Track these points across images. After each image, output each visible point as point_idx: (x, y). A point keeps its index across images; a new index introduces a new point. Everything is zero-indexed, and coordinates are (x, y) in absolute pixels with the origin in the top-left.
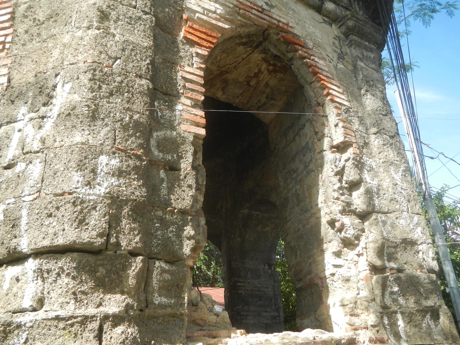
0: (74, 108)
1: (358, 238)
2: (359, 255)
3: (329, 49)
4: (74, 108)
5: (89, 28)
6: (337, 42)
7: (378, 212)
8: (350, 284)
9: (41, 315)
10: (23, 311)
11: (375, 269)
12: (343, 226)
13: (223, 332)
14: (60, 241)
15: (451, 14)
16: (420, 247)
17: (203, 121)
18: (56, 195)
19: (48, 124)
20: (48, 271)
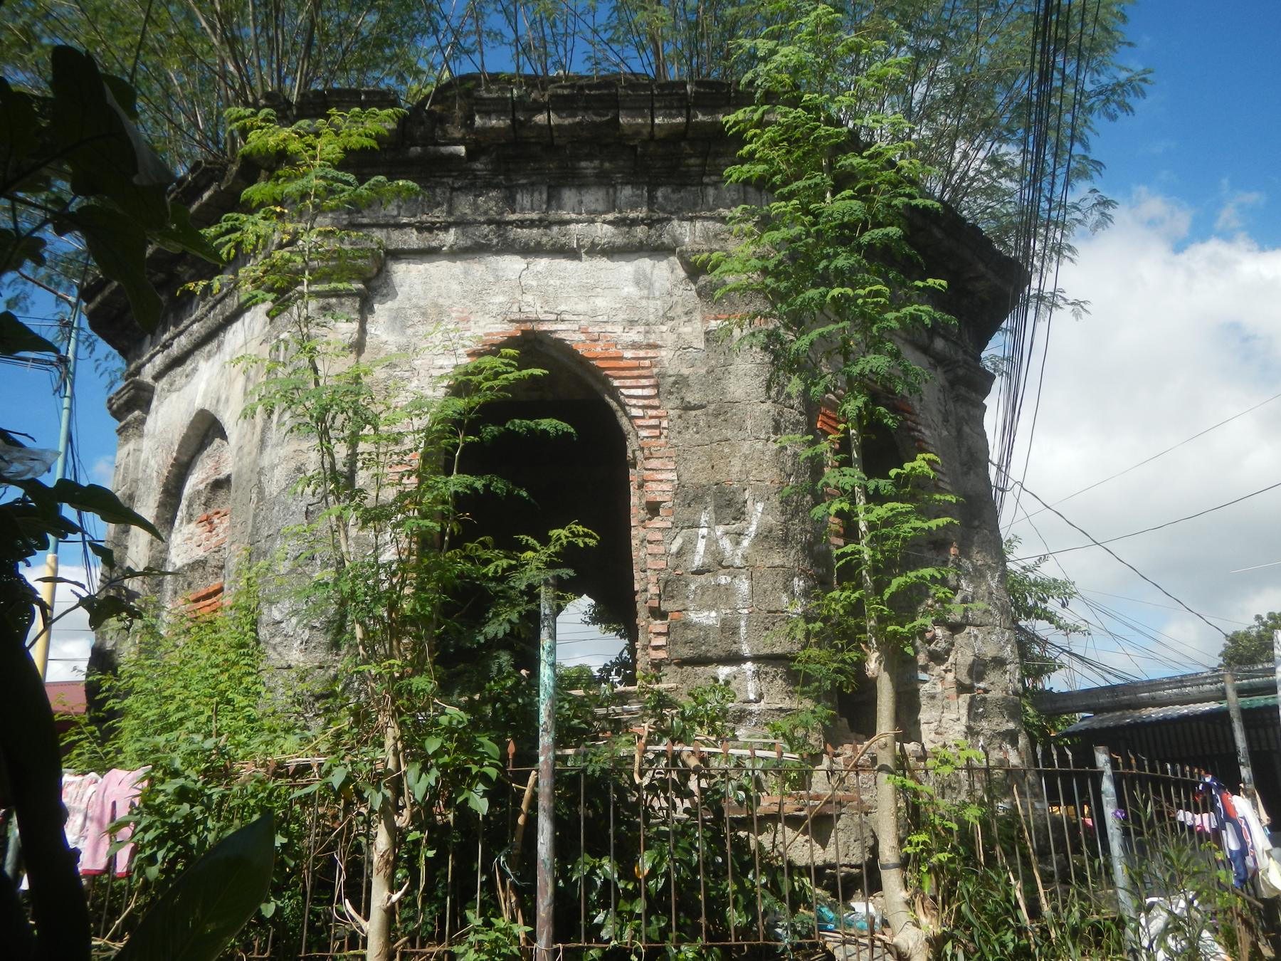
0: (770, 531)
1: (948, 652)
2: (946, 671)
4: (770, 531)
5: (768, 440)
7: (970, 625)
8: (935, 701)
9: (762, 705)
10: (750, 702)
11: (962, 688)
12: (934, 637)
13: (852, 735)
14: (778, 650)
15: (1077, 315)
17: (842, 531)
18: (769, 612)
19: (746, 543)
20: (766, 673)
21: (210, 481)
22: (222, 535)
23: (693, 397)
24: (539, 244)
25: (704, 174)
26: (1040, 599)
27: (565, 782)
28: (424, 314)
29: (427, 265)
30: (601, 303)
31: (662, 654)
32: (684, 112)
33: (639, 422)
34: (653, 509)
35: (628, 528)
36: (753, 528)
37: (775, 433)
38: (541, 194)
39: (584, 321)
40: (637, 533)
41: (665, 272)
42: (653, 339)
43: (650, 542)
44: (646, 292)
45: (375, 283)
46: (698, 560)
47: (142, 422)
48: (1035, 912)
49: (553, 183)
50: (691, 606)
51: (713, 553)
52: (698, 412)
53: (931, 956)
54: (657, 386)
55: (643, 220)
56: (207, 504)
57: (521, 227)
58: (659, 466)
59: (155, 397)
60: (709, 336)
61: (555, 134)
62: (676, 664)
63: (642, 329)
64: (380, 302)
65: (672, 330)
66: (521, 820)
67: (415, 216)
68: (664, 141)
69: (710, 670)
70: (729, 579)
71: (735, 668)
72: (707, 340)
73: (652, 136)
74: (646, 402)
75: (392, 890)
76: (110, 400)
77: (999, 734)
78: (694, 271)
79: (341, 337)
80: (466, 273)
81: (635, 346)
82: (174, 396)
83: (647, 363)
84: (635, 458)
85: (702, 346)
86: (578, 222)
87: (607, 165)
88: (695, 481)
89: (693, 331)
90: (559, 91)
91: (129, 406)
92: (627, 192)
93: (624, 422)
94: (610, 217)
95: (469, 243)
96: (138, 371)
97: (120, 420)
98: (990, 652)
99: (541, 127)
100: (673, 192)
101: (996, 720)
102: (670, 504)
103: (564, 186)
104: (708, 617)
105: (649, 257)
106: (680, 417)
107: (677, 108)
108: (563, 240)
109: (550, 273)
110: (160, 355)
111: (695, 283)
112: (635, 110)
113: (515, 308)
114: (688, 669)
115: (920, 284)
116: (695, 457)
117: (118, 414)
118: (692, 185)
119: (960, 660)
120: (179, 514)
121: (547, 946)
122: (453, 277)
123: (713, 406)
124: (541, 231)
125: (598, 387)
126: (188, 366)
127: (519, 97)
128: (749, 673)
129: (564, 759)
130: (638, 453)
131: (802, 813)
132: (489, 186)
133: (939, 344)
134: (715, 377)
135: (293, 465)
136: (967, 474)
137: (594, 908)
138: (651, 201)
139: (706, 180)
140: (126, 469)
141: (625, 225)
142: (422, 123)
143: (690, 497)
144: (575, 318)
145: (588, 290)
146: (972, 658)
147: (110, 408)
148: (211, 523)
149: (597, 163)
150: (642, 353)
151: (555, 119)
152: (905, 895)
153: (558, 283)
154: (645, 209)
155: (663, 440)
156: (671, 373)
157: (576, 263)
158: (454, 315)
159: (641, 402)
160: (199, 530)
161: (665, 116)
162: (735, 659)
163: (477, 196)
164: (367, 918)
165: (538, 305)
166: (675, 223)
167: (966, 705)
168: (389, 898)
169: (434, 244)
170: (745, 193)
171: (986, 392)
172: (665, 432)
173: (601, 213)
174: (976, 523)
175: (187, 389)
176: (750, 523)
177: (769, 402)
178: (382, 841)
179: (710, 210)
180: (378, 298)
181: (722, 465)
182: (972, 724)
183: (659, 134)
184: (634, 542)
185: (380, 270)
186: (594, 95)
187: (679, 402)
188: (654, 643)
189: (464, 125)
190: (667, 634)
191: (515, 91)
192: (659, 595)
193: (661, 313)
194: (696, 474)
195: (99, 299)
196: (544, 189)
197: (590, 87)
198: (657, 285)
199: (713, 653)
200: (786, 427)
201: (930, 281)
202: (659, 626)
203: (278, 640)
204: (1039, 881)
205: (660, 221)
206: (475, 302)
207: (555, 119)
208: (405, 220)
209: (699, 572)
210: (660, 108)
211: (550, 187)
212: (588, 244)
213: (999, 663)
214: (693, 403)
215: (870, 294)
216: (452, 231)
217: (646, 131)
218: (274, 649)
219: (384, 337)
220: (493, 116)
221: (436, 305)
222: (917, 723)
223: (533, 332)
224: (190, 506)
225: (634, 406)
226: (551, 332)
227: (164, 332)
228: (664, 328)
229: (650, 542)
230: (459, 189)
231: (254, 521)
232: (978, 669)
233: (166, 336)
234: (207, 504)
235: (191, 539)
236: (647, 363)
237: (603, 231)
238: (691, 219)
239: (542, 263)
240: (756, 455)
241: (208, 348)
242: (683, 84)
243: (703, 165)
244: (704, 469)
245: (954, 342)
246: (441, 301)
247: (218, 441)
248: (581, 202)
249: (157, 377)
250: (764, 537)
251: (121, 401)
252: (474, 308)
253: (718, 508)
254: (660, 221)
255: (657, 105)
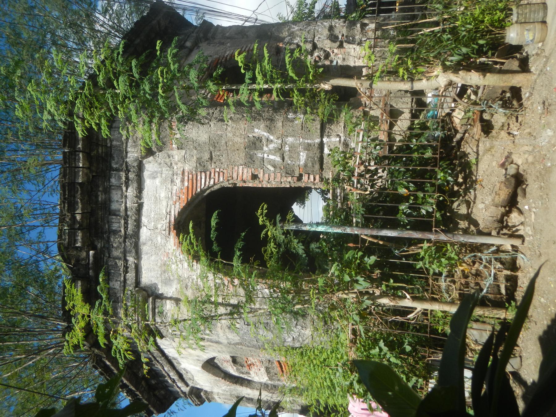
0: (267, 126)
1: (325, 51)
2: (333, 53)
3: (218, 48)
4: (267, 126)
5: (227, 125)
6: (212, 45)
7: (314, 40)
8: (346, 58)
10: (340, 140)
11: (341, 46)
12: (318, 56)
14: (319, 127)
16: (333, 24)
18: (302, 129)
19: (272, 138)
20: (328, 132)
21: (232, 364)
22: (256, 360)
23: (207, 156)
24: (135, 220)
25: (106, 146)
26: (306, 6)
27: (366, 223)
28: (164, 272)
29: (143, 270)
30: (163, 195)
31: (317, 177)
32: (77, 153)
33: (216, 181)
34: (255, 177)
35: (262, 188)
36: (265, 134)
37: (224, 121)
38: (113, 219)
39: (171, 202)
40: (265, 185)
41: (150, 166)
42: (180, 172)
43: (269, 179)
44: (159, 175)
45: (150, 292)
46: (278, 159)
47: (206, 392)
48: (437, 24)
49: (108, 213)
50: (298, 163)
51: (275, 152)
52: (213, 155)
53: (451, 71)
54: (201, 172)
55: (126, 174)
56: (242, 366)
57: (128, 228)
58: (236, 173)
59: (196, 386)
60: (180, 148)
61: (86, 211)
62: (322, 171)
63: (175, 177)
64: (158, 291)
65: (176, 164)
66: (381, 243)
67: (121, 274)
68: (91, 163)
69: (325, 157)
70: (287, 146)
71: (325, 146)
72: (181, 149)
73: (88, 168)
74: (208, 177)
75: (406, 297)
76: (196, 405)
77: (362, 31)
78: (150, 152)
79: (173, 308)
80: (147, 254)
81: (183, 181)
82: (195, 378)
83: (190, 176)
84: (232, 184)
85: (184, 151)
86: (126, 203)
87: (101, 189)
88: (243, 158)
89: (177, 155)
90: (66, 208)
91: (199, 397)
92: (113, 181)
93: (216, 187)
94: (124, 189)
95: (134, 251)
96: (184, 393)
97: (205, 401)
98: (326, 32)
99: (82, 218)
100: (114, 160)
101: (356, 32)
102: (253, 169)
103: (110, 208)
104: (303, 156)
105: (143, 172)
106: (215, 163)
107: (75, 155)
108: (134, 210)
109: (148, 216)
110: (178, 384)
111: (156, 153)
112: (76, 175)
113: (164, 232)
114: (324, 166)
115: (158, 53)
116: (233, 157)
117: (202, 402)
118: (111, 151)
119: (329, 46)
120: (246, 378)
121: (433, 235)
122: (148, 259)
123: (211, 148)
124: (129, 219)
125: (200, 198)
126: (183, 372)
127: (68, 226)
128: (328, 140)
129: (357, 223)
130: (230, 182)
131: (388, 121)
132: (108, 241)
133: (188, 44)
134: (198, 146)
135: (227, 330)
136: (247, 36)
137: (420, 213)
138: (118, 170)
139: (109, 145)
140: (225, 399)
141: (128, 182)
142: (79, 269)
143: (250, 160)
144: (169, 206)
145: (157, 200)
146: (328, 41)
147: (199, 405)
148: (250, 365)
149: (99, 193)
150: (186, 178)
151: (79, 211)
152: (424, 81)
153: (153, 213)
154: (121, 173)
155: (225, 171)
156: (195, 165)
157: (144, 205)
158: (165, 259)
159: (208, 180)
160: (253, 370)
161: (79, 162)
162: (321, 146)
163: (113, 247)
164: (416, 309)
165: (162, 222)
166: (128, 160)
167: (349, 45)
168: (408, 299)
169: (133, 266)
170: (115, 128)
171: (211, 24)
172: (221, 170)
173: (122, 192)
174: (269, 33)
175: (193, 373)
176: (263, 135)
177: (210, 123)
178: (385, 301)
179: (123, 144)
180: (156, 291)
181: (237, 146)
182: (357, 43)
183: (87, 165)
184: (269, 186)
185: (144, 290)
186: (68, 193)
187: (208, 163)
188: (312, 180)
189: (81, 251)
190: (309, 174)
191: (66, 228)
192: (292, 177)
193: (168, 168)
194: (240, 157)
195: (152, 409)
196: (111, 217)
197: (64, 195)
198: (156, 169)
199: (318, 155)
200: (222, 116)
201: (158, 48)
202: (305, 178)
203: (300, 339)
204: (423, 21)
205: (127, 166)
206: (160, 250)
207: (79, 211)
208: (122, 278)
209: (283, 159)
210: (75, 164)
211: (110, 215)
212: (136, 199)
213: (331, 28)
214: (209, 157)
215: (162, 76)
216: (128, 258)
217: (85, 171)
218: (304, 341)
219: (174, 289)
220: (77, 238)
221: (160, 267)
222: (355, 67)
223: (174, 225)
224: (243, 373)
225: (209, 182)
226: (175, 217)
227: (167, 382)
228: (175, 167)
229: (269, 179)
230: (109, 254)
231: (250, 347)
232: (333, 38)
233: (169, 381)
234: (242, 366)
235: (257, 373)
236: (190, 176)
237: (131, 192)
238: (127, 153)
239: (144, 220)
240: (233, 131)
241: (175, 364)
242: (64, 153)
243: (102, 146)
244: (238, 154)
245: (188, 38)
246: (159, 264)
247: (216, 361)
248: (117, 201)
249: (187, 385)
250: (269, 129)
251: (197, 400)
252: (163, 250)
253: (256, 148)
254: (127, 166)
255: (74, 165)
